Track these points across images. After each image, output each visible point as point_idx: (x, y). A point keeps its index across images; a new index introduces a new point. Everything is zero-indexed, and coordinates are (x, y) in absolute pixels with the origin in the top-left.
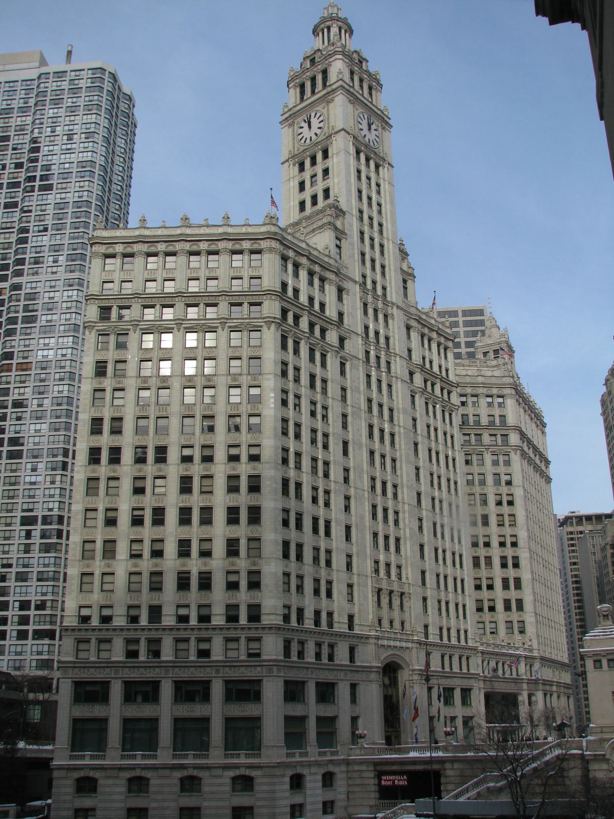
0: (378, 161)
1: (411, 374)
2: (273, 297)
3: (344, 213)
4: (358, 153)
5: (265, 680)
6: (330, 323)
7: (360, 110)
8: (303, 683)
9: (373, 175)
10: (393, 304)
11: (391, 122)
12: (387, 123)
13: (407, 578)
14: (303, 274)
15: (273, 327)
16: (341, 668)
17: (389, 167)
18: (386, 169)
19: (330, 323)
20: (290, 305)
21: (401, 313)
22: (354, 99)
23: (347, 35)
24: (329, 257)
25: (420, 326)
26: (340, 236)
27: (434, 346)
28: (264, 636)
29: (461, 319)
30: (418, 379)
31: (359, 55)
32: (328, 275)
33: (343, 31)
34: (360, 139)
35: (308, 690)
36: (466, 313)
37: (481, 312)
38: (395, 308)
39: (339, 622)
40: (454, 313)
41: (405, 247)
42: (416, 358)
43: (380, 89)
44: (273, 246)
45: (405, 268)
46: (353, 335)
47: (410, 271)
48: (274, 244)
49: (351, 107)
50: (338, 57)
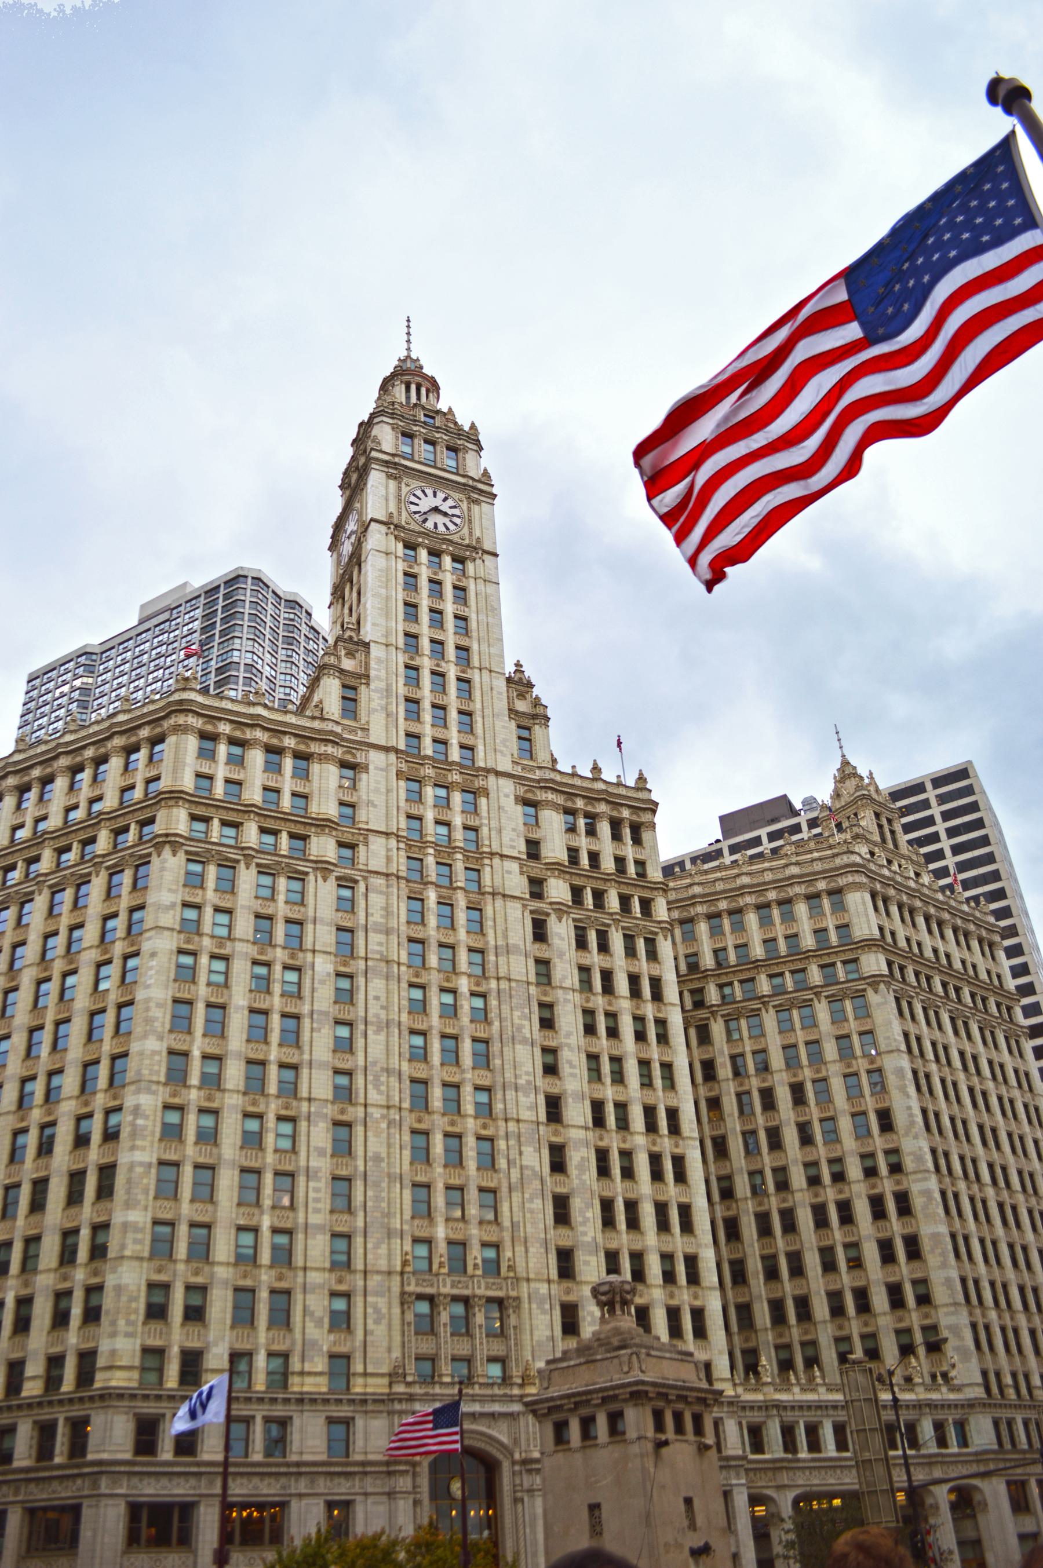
0: (460, 553)
1: (537, 887)
2: (171, 803)
3: (366, 645)
4: (410, 546)
5: (86, 1503)
6: (311, 824)
7: (415, 484)
8: (187, 1509)
9: (448, 581)
10: (488, 771)
11: (495, 491)
12: (482, 492)
13: (510, 1268)
14: (256, 757)
15: (167, 851)
16: (300, 1470)
17: (486, 557)
18: (478, 562)
19: (311, 824)
20: (213, 810)
21: (507, 787)
22: (395, 469)
23: (423, 391)
24: (323, 719)
25: (560, 800)
26: (352, 682)
27: (604, 828)
28: (92, 1413)
29: (931, 794)
30: (558, 890)
31: (424, 408)
32: (315, 748)
33: (413, 387)
34: (414, 526)
35: (198, 1522)
36: (938, 781)
37: (962, 773)
38: (492, 778)
39: (302, 1373)
40: (918, 788)
41: (526, 674)
42: (555, 850)
43: (475, 447)
44: (181, 722)
45: (522, 706)
46: (372, 838)
47: (540, 710)
48: (181, 719)
49: (392, 484)
50: (376, 420)
